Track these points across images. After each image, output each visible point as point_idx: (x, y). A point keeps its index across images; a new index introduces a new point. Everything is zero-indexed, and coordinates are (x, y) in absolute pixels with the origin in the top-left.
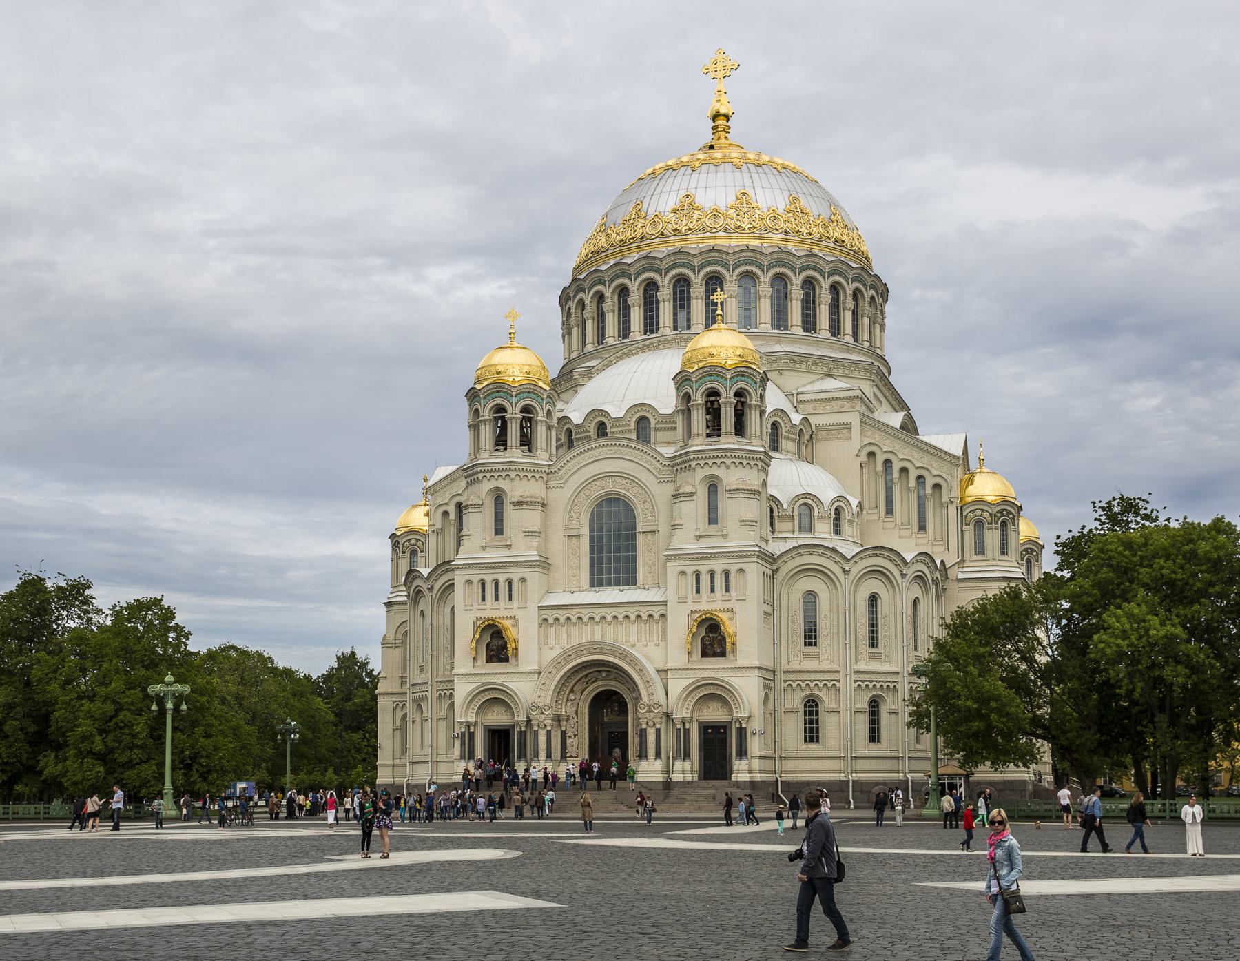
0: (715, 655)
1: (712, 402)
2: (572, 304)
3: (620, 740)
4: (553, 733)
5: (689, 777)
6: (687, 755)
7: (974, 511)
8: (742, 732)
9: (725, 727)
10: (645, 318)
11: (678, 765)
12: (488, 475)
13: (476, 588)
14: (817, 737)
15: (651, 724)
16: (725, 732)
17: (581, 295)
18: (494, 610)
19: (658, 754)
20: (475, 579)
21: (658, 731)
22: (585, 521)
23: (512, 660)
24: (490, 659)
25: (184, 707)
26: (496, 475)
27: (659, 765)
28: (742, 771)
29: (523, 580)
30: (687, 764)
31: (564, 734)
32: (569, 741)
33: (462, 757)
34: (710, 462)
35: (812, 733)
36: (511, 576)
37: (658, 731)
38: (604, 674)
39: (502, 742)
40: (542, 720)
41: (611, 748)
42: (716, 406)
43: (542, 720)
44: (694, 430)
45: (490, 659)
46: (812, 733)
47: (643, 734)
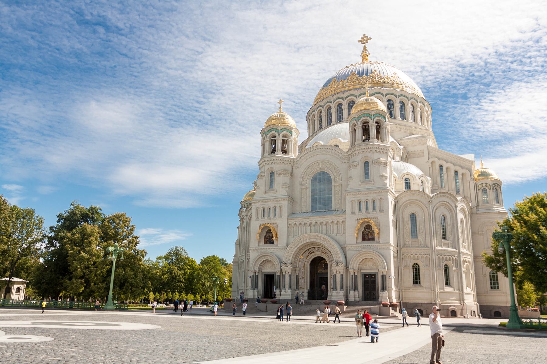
0: (369, 239)
1: (365, 126)
2: (310, 118)
3: (324, 281)
4: (292, 277)
5: (357, 299)
6: (356, 289)
7: (482, 184)
8: (383, 277)
9: (375, 275)
10: (337, 116)
11: (352, 293)
12: (267, 163)
13: (261, 211)
14: (420, 282)
15: (338, 272)
16: (375, 277)
17: (314, 113)
18: (268, 221)
19: (342, 288)
20: (261, 207)
21: (342, 275)
22: (309, 181)
23: (275, 242)
24: (266, 243)
25: (122, 258)
26: (271, 162)
27: (342, 293)
28: (384, 297)
29: (281, 207)
30: (356, 293)
31: (298, 277)
32: (300, 281)
33: (252, 287)
34: (365, 151)
35: (417, 281)
36: (276, 205)
37: (342, 275)
38: (316, 249)
39: (269, 279)
40: (288, 270)
41: (321, 284)
42: (367, 127)
43: (288, 270)
44: (357, 138)
45: (266, 243)
46: (417, 281)
47: (335, 277)
